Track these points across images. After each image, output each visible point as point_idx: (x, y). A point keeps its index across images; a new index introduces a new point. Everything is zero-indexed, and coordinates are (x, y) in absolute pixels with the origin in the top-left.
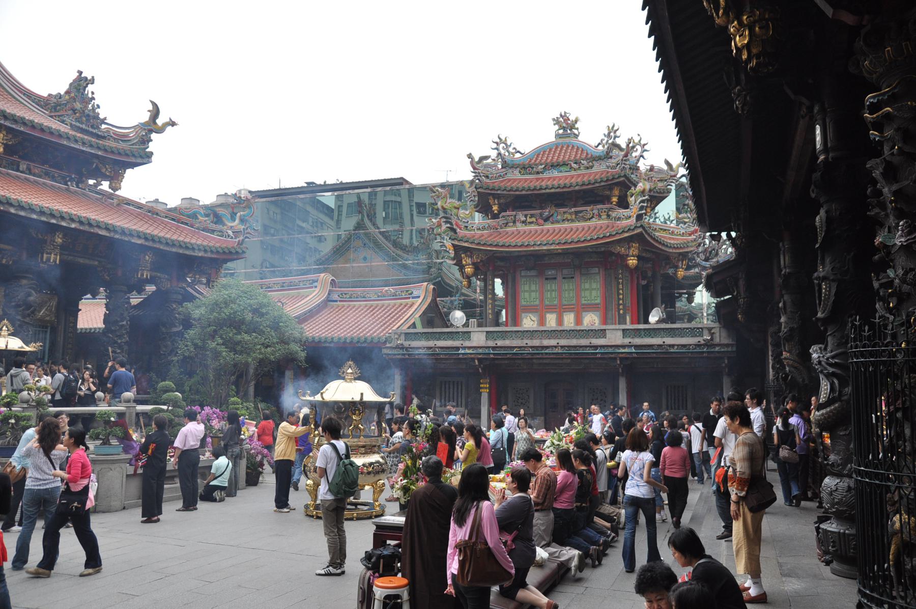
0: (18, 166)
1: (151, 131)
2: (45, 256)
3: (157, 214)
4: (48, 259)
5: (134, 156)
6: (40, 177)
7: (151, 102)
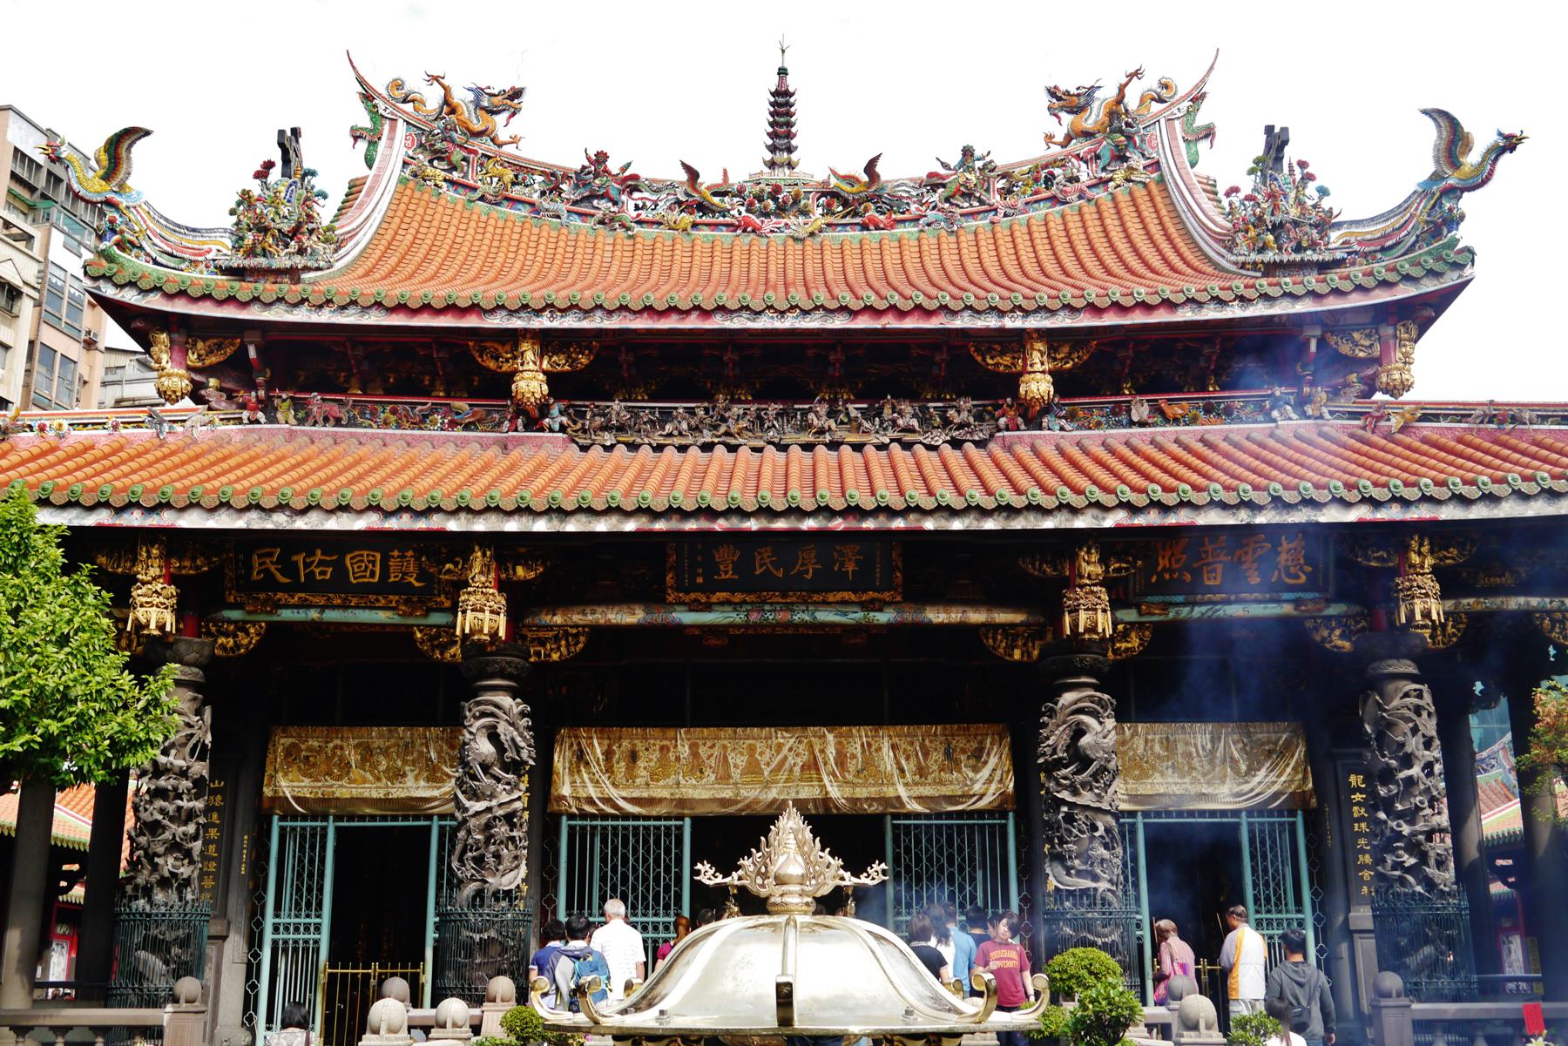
0: (1129, 411)
1: (1454, 192)
2: (1067, 619)
3: (1514, 419)
4: (1075, 625)
5: (1407, 278)
6: (1194, 421)
7: (1425, 112)
